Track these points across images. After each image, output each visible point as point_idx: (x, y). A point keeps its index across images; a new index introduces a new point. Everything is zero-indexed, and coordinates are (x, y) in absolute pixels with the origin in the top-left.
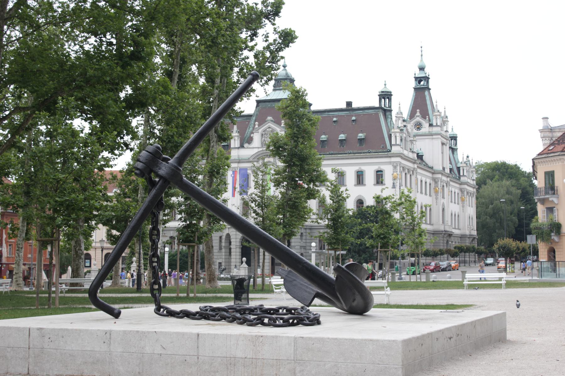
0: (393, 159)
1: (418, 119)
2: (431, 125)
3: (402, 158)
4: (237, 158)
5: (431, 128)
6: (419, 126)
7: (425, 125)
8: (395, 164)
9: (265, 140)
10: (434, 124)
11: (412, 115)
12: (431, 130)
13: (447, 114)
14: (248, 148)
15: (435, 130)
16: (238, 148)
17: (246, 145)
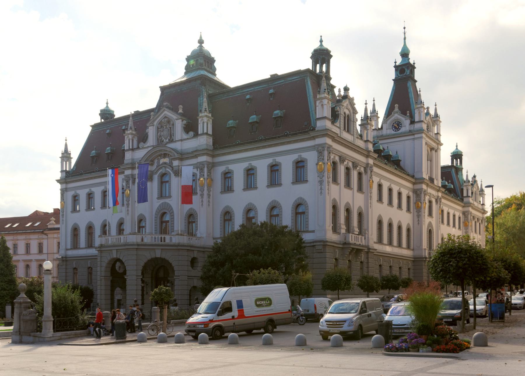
0: (319, 141)
1: (397, 116)
2: (412, 122)
3: (334, 140)
4: (130, 161)
5: (412, 126)
6: (397, 125)
7: (406, 122)
8: (320, 148)
9: (160, 136)
10: (417, 119)
11: (389, 112)
12: (412, 129)
13: (439, 113)
14: (143, 148)
15: (417, 126)
16: (133, 150)
17: (141, 145)
